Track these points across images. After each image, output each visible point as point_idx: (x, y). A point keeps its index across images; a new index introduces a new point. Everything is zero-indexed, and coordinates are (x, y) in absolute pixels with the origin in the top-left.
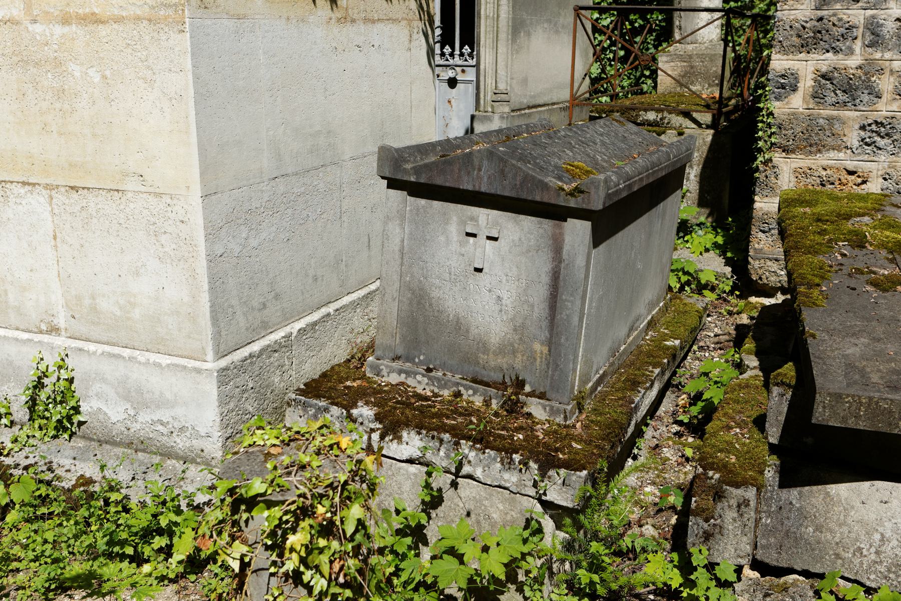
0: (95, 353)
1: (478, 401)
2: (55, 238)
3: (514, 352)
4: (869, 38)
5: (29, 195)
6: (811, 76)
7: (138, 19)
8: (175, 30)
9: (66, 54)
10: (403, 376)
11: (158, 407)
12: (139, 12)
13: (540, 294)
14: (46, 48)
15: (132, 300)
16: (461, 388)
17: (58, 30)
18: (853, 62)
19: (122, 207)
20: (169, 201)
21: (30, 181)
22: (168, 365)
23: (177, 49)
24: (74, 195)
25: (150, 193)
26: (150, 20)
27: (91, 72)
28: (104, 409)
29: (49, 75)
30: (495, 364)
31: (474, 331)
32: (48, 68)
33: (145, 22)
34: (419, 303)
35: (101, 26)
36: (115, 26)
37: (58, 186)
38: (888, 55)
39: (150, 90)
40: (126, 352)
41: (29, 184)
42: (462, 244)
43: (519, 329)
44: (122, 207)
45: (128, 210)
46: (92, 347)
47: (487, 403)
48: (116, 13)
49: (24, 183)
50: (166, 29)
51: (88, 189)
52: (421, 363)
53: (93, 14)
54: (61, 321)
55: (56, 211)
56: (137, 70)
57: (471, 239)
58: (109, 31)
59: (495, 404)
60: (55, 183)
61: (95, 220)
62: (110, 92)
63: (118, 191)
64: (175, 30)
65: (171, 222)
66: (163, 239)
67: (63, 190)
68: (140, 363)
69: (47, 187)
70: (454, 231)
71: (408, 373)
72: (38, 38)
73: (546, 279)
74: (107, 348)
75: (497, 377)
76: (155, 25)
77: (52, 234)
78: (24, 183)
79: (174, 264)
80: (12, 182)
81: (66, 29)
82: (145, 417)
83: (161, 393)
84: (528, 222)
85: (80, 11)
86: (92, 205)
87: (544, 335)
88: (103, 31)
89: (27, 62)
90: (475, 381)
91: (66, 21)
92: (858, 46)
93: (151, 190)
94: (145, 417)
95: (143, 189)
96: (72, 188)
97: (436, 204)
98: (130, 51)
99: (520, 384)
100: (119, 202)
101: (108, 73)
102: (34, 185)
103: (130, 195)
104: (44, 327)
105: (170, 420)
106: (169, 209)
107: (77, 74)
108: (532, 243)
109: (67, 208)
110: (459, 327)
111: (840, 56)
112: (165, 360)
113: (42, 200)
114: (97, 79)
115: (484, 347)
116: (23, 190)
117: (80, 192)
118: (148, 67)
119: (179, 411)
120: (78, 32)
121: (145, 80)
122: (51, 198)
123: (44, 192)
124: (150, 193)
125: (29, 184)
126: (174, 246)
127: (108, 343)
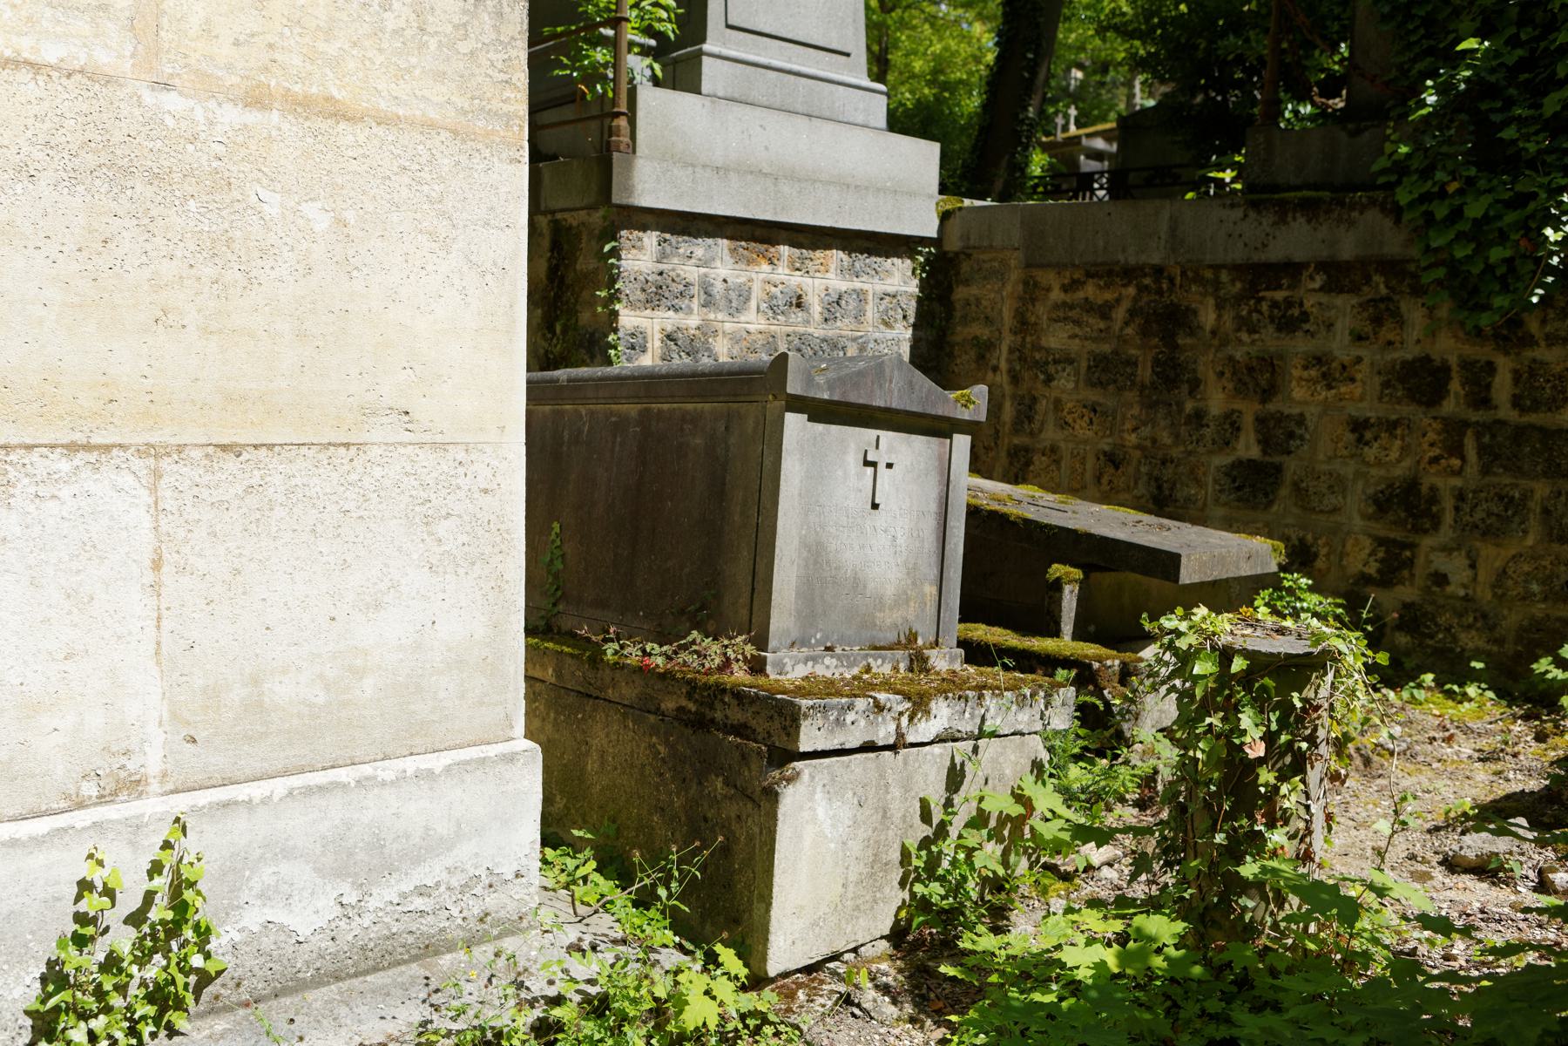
0: (266, 801)
1: (887, 669)
2: (157, 565)
3: (907, 601)
4: (703, 297)
5: (86, 473)
6: (658, 336)
7: (429, 126)
8: (504, 156)
9: (246, 167)
10: (810, 664)
11: (417, 861)
12: (433, 114)
13: (929, 525)
14: (190, 148)
15: (359, 662)
16: (870, 660)
17: (231, 116)
18: (693, 321)
19: (354, 477)
20: (461, 456)
21: (97, 439)
22: (448, 769)
23: (503, 189)
24: (231, 463)
25: (421, 445)
26: (455, 133)
27: (310, 209)
28: (280, 917)
29: (192, 204)
30: (890, 622)
31: (871, 585)
32: (190, 190)
33: (444, 135)
34: (816, 562)
35: (343, 125)
36: (380, 131)
37: (180, 448)
38: (720, 316)
39: (442, 254)
40: (342, 775)
41: (88, 448)
42: (860, 476)
43: (912, 571)
44: (354, 477)
45: (367, 481)
46: (256, 791)
47: (896, 669)
48: (383, 105)
49: (72, 448)
50: (487, 153)
51: (270, 447)
52: (818, 643)
53: (329, 98)
54: (153, 762)
55: (169, 504)
56: (418, 216)
57: (870, 470)
58: (361, 138)
59: (902, 666)
60: (174, 441)
61: (279, 512)
62: (351, 252)
63: (347, 445)
64: (504, 156)
65: (460, 494)
66: (442, 528)
67: (197, 454)
68: (384, 784)
69: (149, 450)
70: (853, 460)
71: (814, 659)
72: (170, 122)
73: (933, 507)
74: (296, 781)
75: (891, 637)
76: (464, 141)
77: (147, 558)
78: (72, 448)
79: (461, 571)
80: (29, 448)
81: (253, 117)
82: (384, 894)
83: (427, 829)
84: (919, 441)
85: (297, 88)
86: (277, 479)
87: (935, 571)
88: (346, 134)
89: (128, 172)
90: (876, 648)
91: (256, 100)
92: (695, 304)
93: (427, 438)
94: (384, 894)
95: (408, 437)
96: (224, 448)
97: (835, 429)
98: (406, 179)
99: (912, 637)
100: (347, 467)
101: (350, 215)
102: (107, 448)
103: (375, 452)
104: (90, 789)
105: (444, 876)
106: (461, 470)
107: (272, 210)
108: (922, 466)
109: (205, 493)
110: (857, 584)
111: (681, 315)
112: (437, 762)
113: (127, 480)
114: (322, 223)
115: (880, 603)
116: (64, 466)
117: (245, 456)
118: (442, 214)
119: (464, 853)
120: (285, 126)
121: (433, 236)
122: (157, 474)
123: (137, 464)
124: (421, 445)
125: (88, 448)
126: (465, 538)
127: (286, 773)
